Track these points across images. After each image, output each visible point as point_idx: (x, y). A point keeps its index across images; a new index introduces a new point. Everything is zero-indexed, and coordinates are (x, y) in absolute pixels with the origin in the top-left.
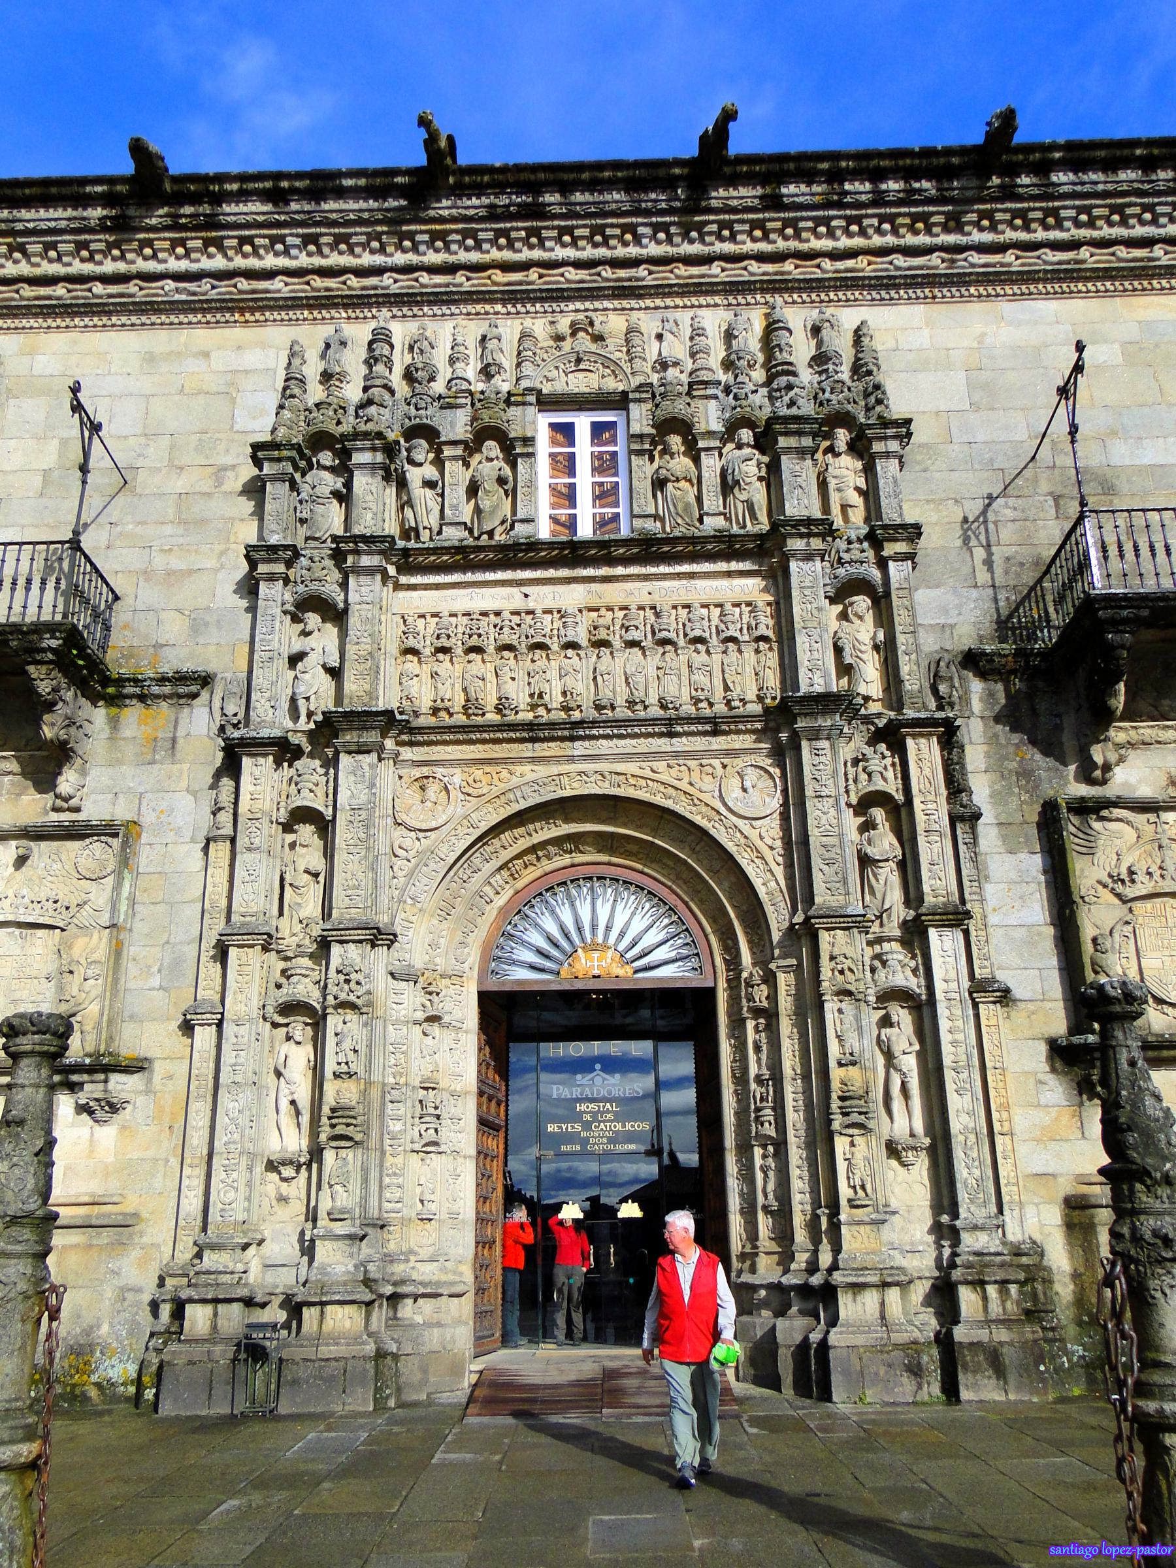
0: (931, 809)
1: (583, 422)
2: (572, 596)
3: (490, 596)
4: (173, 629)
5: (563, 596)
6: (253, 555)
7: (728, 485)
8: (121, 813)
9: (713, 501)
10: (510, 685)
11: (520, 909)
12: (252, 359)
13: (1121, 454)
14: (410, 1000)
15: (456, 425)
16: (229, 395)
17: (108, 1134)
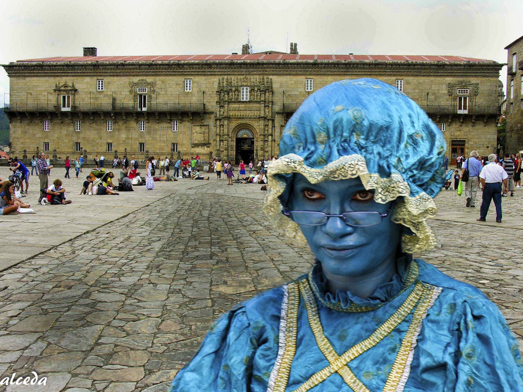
0: (270, 126)
1: (245, 88)
2: (243, 105)
3: (236, 105)
4: (210, 107)
5: (242, 106)
6: (217, 102)
7: (257, 96)
8: (207, 124)
9: (256, 97)
10: (238, 113)
11: (239, 131)
12: (215, 80)
13: (293, 93)
14: (230, 139)
15: (234, 89)
16: (213, 83)
17: (208, 149)
